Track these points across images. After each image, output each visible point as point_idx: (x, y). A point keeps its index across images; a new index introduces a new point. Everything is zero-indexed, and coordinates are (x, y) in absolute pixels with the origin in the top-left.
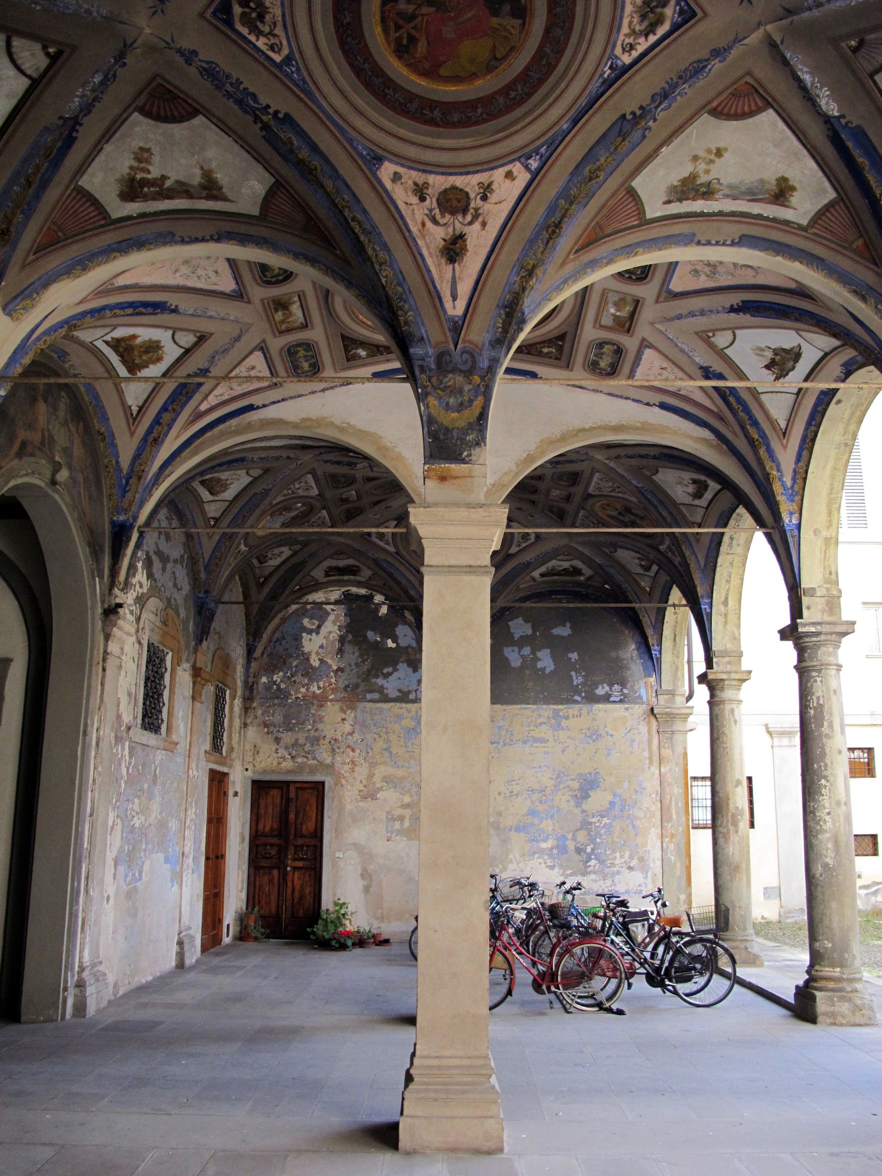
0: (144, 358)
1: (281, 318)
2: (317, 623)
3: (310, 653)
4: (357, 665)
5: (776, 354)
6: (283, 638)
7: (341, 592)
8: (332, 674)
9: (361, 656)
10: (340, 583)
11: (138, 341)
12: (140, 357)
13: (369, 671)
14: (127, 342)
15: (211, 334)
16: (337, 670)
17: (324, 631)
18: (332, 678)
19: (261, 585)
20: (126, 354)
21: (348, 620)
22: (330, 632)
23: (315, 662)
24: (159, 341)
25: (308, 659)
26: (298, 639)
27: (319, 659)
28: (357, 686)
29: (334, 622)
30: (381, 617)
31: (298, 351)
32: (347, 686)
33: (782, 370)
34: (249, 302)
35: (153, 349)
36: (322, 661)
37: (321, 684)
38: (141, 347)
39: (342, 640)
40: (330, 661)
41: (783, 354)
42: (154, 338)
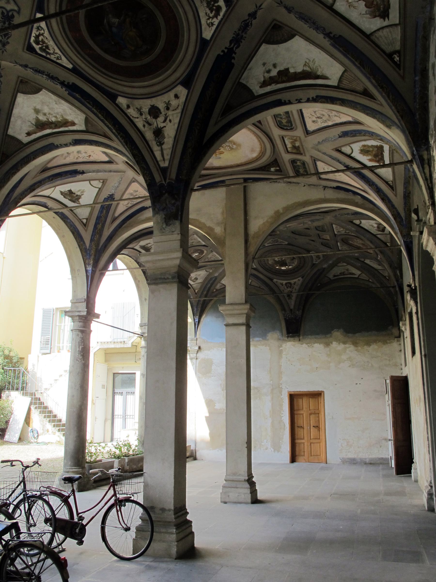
0: (371, 149)
1: (296, 143)
5: (77, 195)
11: (370, 157)
12: (373, 150)
14: (375, 159)
15: (333, 150)
20: (380, 154)
24: (360, 153)
31: (287, 122)
33: (66, 194)
34: (311, 157)
35: (365, 151)
38: (370, 154)
41: (77, 197)
42: (361, 155)
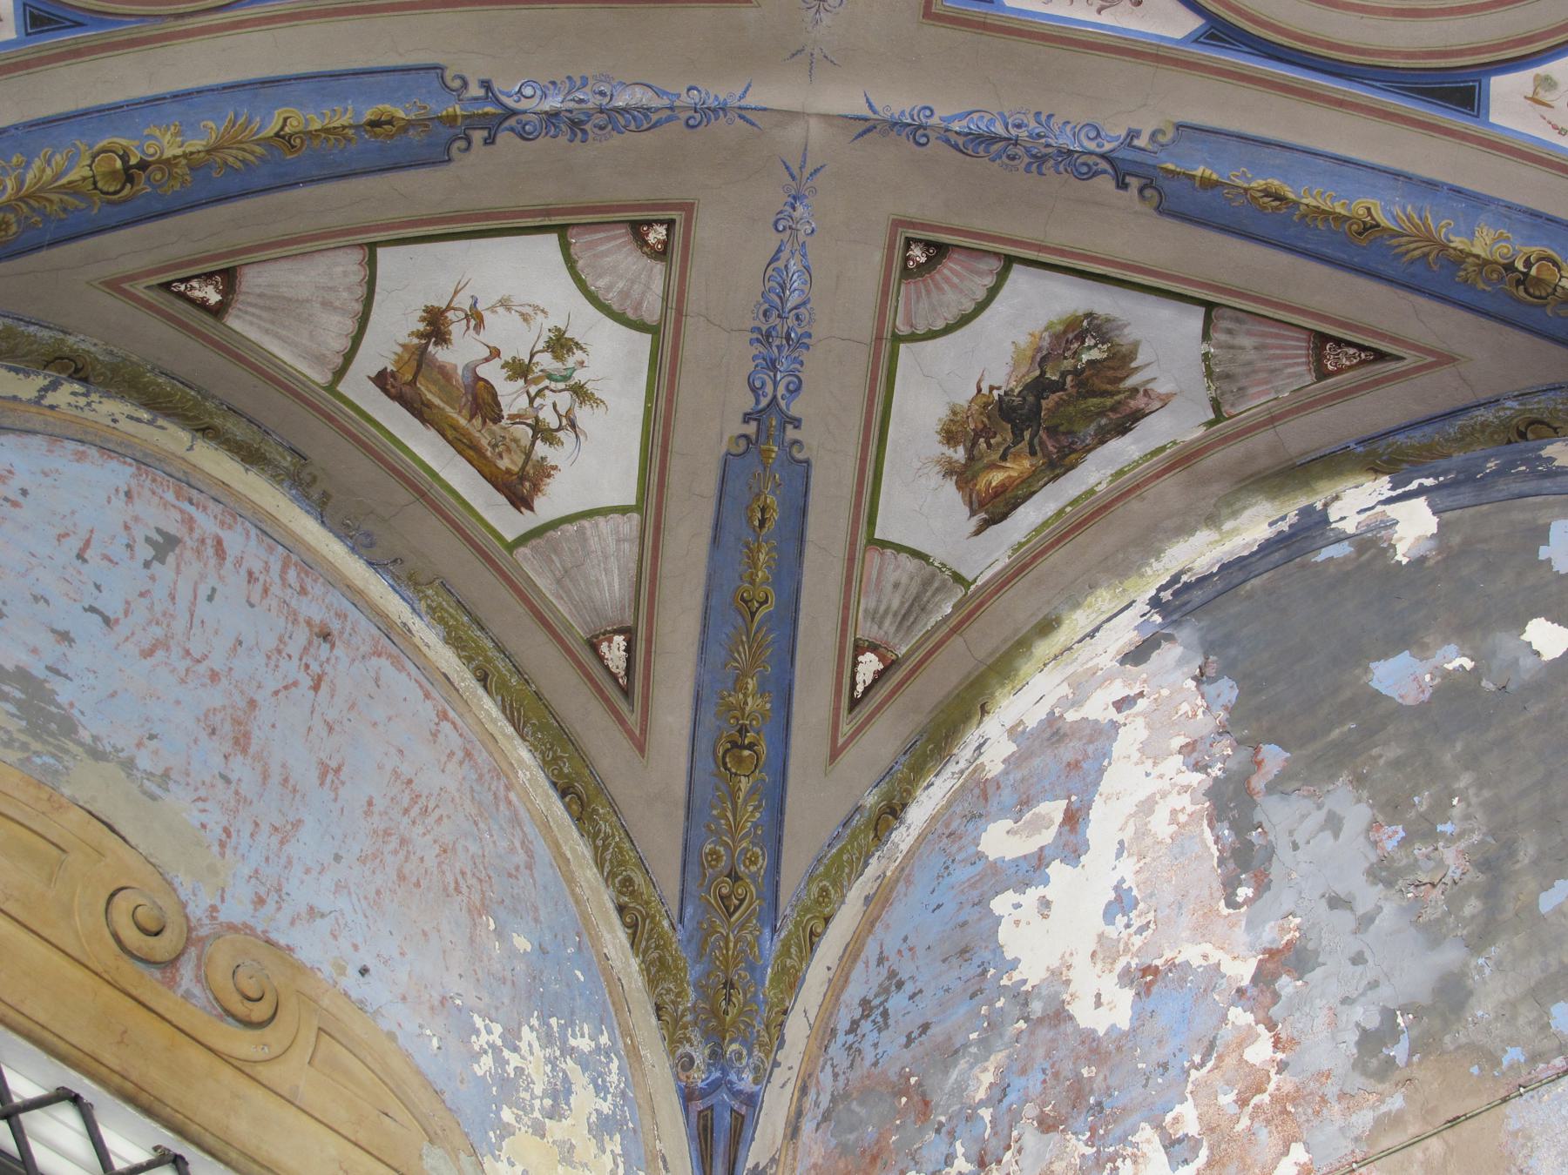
2: (1054, 810)
3: (1059, 976)
4: (1384, 873)
6: (895, 982)
7: (1142, 606)
8: (1240, 1017)
9: (1392, 807)
10: (1120, 566)
13: (1493, 866)
16: (1264, 978)
17: (1103, 824)
18: (1247, 1038)
19: (628, 690)
21: (1227, 691)
22: (1147, 806)
23: (1102, 1006)
25: (1059, 1015)
26: (972, 948)
27: (1126, 978)
28: (1452, 995)
29: (1151, 752)
30: (1419, 562)
32: (1371, 1041)
36: (1145, 979)
37: (1187, 1117)
39: (1231, 803)
40: (1192, 954)
